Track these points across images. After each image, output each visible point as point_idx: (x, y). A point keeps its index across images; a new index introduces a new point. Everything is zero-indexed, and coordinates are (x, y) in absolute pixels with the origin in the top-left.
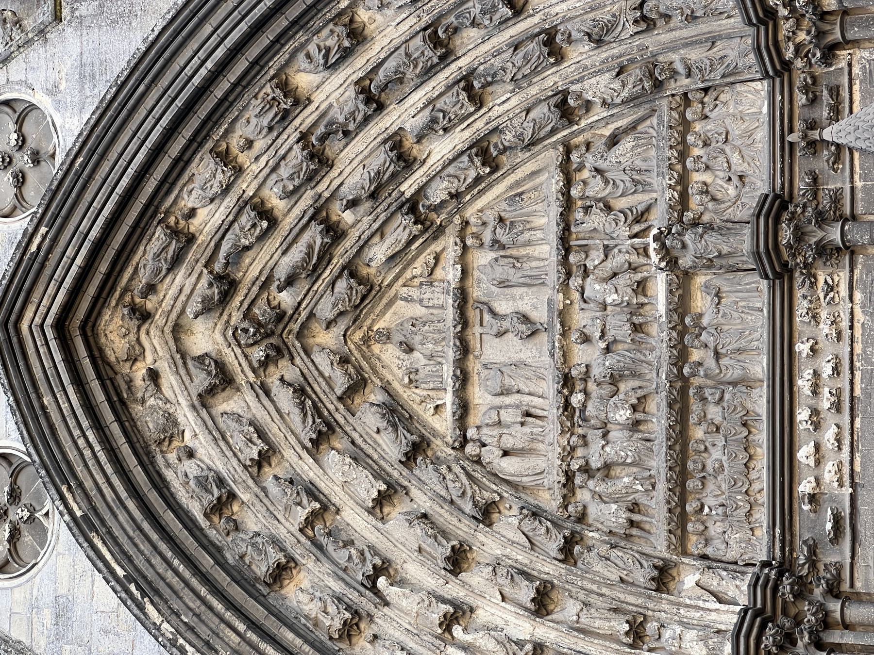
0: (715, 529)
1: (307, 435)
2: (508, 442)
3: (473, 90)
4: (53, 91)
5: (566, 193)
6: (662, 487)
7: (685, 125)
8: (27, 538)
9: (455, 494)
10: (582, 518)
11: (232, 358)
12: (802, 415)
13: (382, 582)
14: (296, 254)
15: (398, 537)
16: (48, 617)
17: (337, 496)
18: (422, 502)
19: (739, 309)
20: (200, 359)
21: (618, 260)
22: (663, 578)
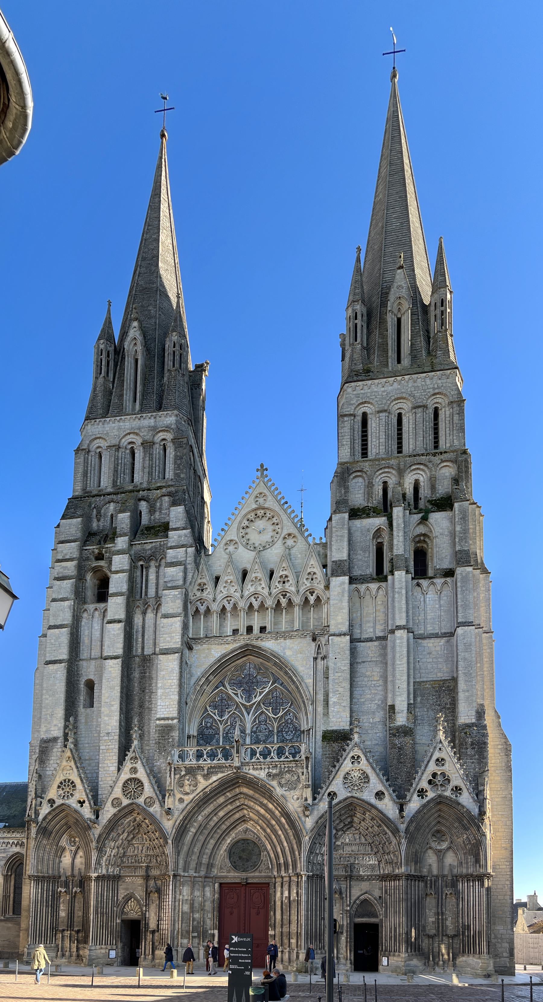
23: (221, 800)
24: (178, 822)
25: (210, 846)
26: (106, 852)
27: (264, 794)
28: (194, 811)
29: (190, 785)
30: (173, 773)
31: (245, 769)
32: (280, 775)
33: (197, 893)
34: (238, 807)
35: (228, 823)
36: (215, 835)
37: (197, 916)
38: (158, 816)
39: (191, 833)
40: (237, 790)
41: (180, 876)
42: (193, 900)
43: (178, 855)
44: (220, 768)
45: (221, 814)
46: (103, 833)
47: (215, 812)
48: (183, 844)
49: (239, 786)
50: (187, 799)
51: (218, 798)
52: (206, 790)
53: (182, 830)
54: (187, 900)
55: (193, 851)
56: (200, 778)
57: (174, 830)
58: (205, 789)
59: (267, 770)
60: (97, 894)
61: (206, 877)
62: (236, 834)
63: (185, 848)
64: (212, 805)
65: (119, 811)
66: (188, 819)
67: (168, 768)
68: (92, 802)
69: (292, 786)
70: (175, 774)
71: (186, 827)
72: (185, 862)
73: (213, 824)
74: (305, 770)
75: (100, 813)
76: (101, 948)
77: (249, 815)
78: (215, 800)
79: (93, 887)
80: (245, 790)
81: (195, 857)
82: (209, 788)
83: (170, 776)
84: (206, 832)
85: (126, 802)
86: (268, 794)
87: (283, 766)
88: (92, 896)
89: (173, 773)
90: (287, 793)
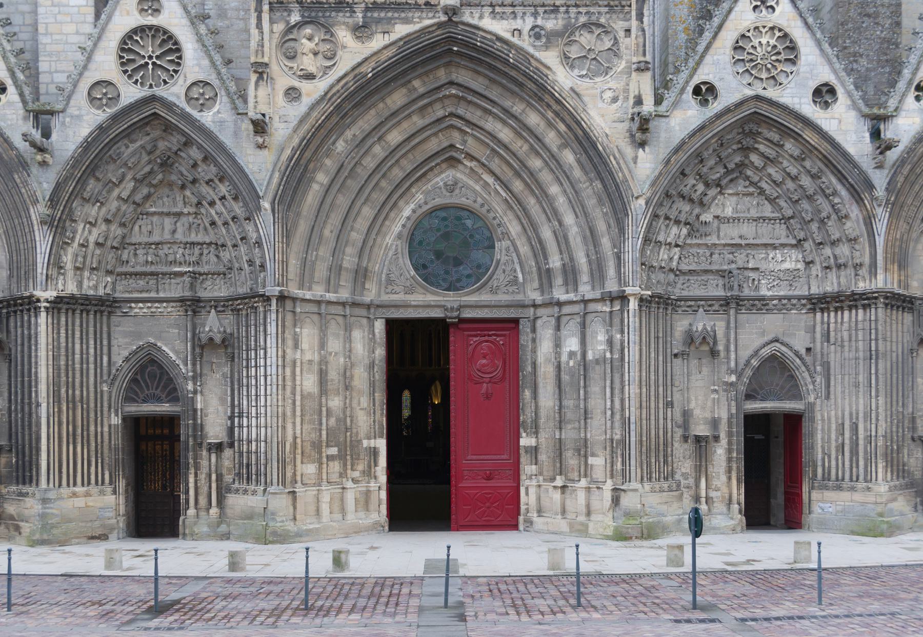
0: (123, 282)
1: (138, 176)
2: (143, 227)
3: (226, 224)
4: (218, 112)
5: (205, 243)
6: (132, 270)
7: (219, 274)
8: (98, 102)
9: (127, 216)
10: (124, 248)
11: (158, 152)
12: (149, 305)
13: (98, 204)
14: (185, 173)
15: (114, 205)
16: (77, 113)
17: (122, 186)
18: (124, 208)
20: (155, 146)
21: (187, 258)
22: (109, 272)
23: (397, 99)
24: (288, 152)
25: (362, 224)
26: (74, 232)
27: (521, 85)
28: (329, 125)
29: (316, 54)
30: (266, 17)
31: (469, 17)
32: (567, 34)
33: (334, 345)
34: (439, 120)
36: (374, 196)
37: (335, 403)
38: (226, 138)
39: (315, 187)
40: (442, 75)
41: (294, 299)
42: (323, 361)
45: (395, 137)
46: (66, 180)
48: (298, 214)
49: (448, 65)
50: (313, 91)
51: (390, 93)
52: (363, 69)
53: (296, 176)
54: (310, 362)
55: (321, 237)
56: (344, 35)
58: (360, 64)
59: (529, 22)
60: (56, 348)
61: (354, 304)
63: (303, 227)
64: (373, 112)
65: (115, 118)
66: (312, 147)
68: (27, 91)
69: (597, 65)
70: (272, 22)
71: (306, 166)
73: (372, 165)
74: (634, 23)
75: (56, 123)
76: (74, 495)
78: (382, 99)
79: (42, 328)
81: (324, 252)
83: (259, 26)
84: (354, 185)
85: (130, 93)
86: (537, 89)
87: (573, 10)
88: (42, 353)
89: (266, 17)
90: (583, 85)
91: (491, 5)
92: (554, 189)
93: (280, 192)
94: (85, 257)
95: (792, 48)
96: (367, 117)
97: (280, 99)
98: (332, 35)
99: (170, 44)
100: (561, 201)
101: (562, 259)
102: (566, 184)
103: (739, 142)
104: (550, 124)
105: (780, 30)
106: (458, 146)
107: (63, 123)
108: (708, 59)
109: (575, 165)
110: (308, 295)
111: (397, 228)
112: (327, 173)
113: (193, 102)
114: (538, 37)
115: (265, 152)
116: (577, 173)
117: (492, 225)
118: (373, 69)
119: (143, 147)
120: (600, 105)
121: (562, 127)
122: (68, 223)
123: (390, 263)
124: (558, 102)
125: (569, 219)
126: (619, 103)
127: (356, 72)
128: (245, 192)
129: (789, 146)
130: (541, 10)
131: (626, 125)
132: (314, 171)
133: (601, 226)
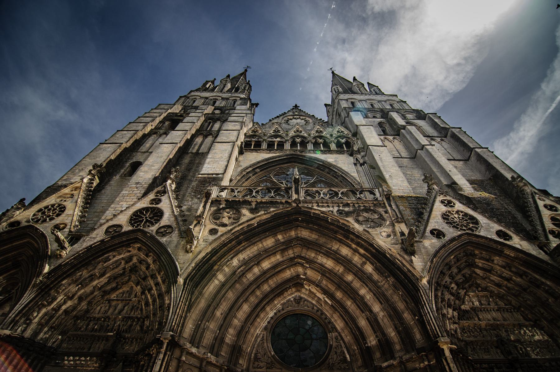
11: (131, 263)
15: (88, 289)
19: (99, 347)
23: (269, 242)
26: (55, 299)
29: (229, 218)
35: (272, 283)
39: (216, 282)
40: (293, 233)
41: (183, 349)
43: (189, 310)
44: (272, 203)
45: (266, 265)
47: (257, 259)
48: (201, 293)
52: (252, 222)
57: (193, 265)
59: (336, 209)
62: (283, 304)
67: (204, 200)
70: (210, 206)
72: (198, 327)
74: (389, 208)
77: (305, 274)
80: (305, 234)
81: (213, 325)
82: (258, 219)
83: (204, 207)
91: (317, 203)
92: (363, 292)
93: (192, 274)
94: (52, 317)
95: (472, 218)
96: (252, 250)
97: (206, 233)
98: (239, 212)
99: (159, 214)
100: (368, 298)
101: (377, 336)
102: (370, 285)
103: (466, 262)
104: (356, 251)
105: (462, 212)
106: (301, 276)
107: (84, 240)
108: (431, 221)
109: (374, 273)
110: (194, 350)
111: (264, 324)
112: (225, 275)
113: (159, 234)
114: (341, 213)
115: (191, 254)
116: (376, 277)
117: (325, 323)
118: (258, 223)
119: (123, 259)
120: (381, 238)
121: (362, 251)
122: (52, 292)
123: (258, 346)
124: (358, 237)
125: (376, 308)
126: (392, 237)
127: (249, 223)
128: (171, 274)
129: (497, 259)
130: (341, 205)
131: (398, 246)
132: (217, 271)
133: (401, 306)
